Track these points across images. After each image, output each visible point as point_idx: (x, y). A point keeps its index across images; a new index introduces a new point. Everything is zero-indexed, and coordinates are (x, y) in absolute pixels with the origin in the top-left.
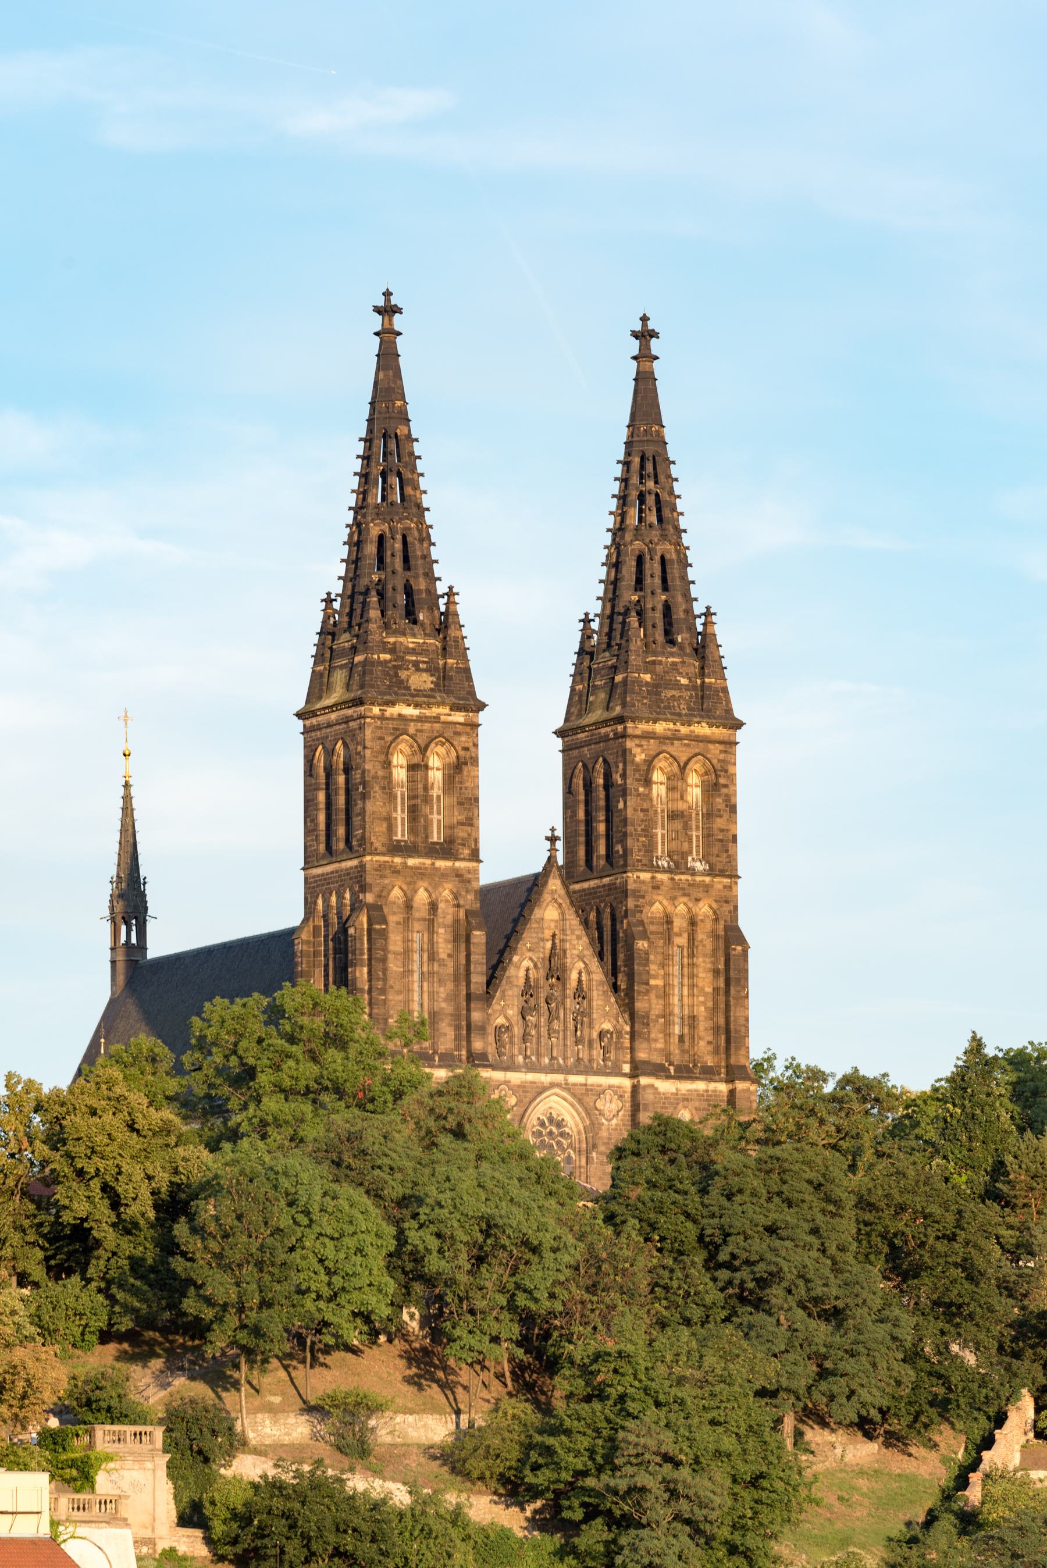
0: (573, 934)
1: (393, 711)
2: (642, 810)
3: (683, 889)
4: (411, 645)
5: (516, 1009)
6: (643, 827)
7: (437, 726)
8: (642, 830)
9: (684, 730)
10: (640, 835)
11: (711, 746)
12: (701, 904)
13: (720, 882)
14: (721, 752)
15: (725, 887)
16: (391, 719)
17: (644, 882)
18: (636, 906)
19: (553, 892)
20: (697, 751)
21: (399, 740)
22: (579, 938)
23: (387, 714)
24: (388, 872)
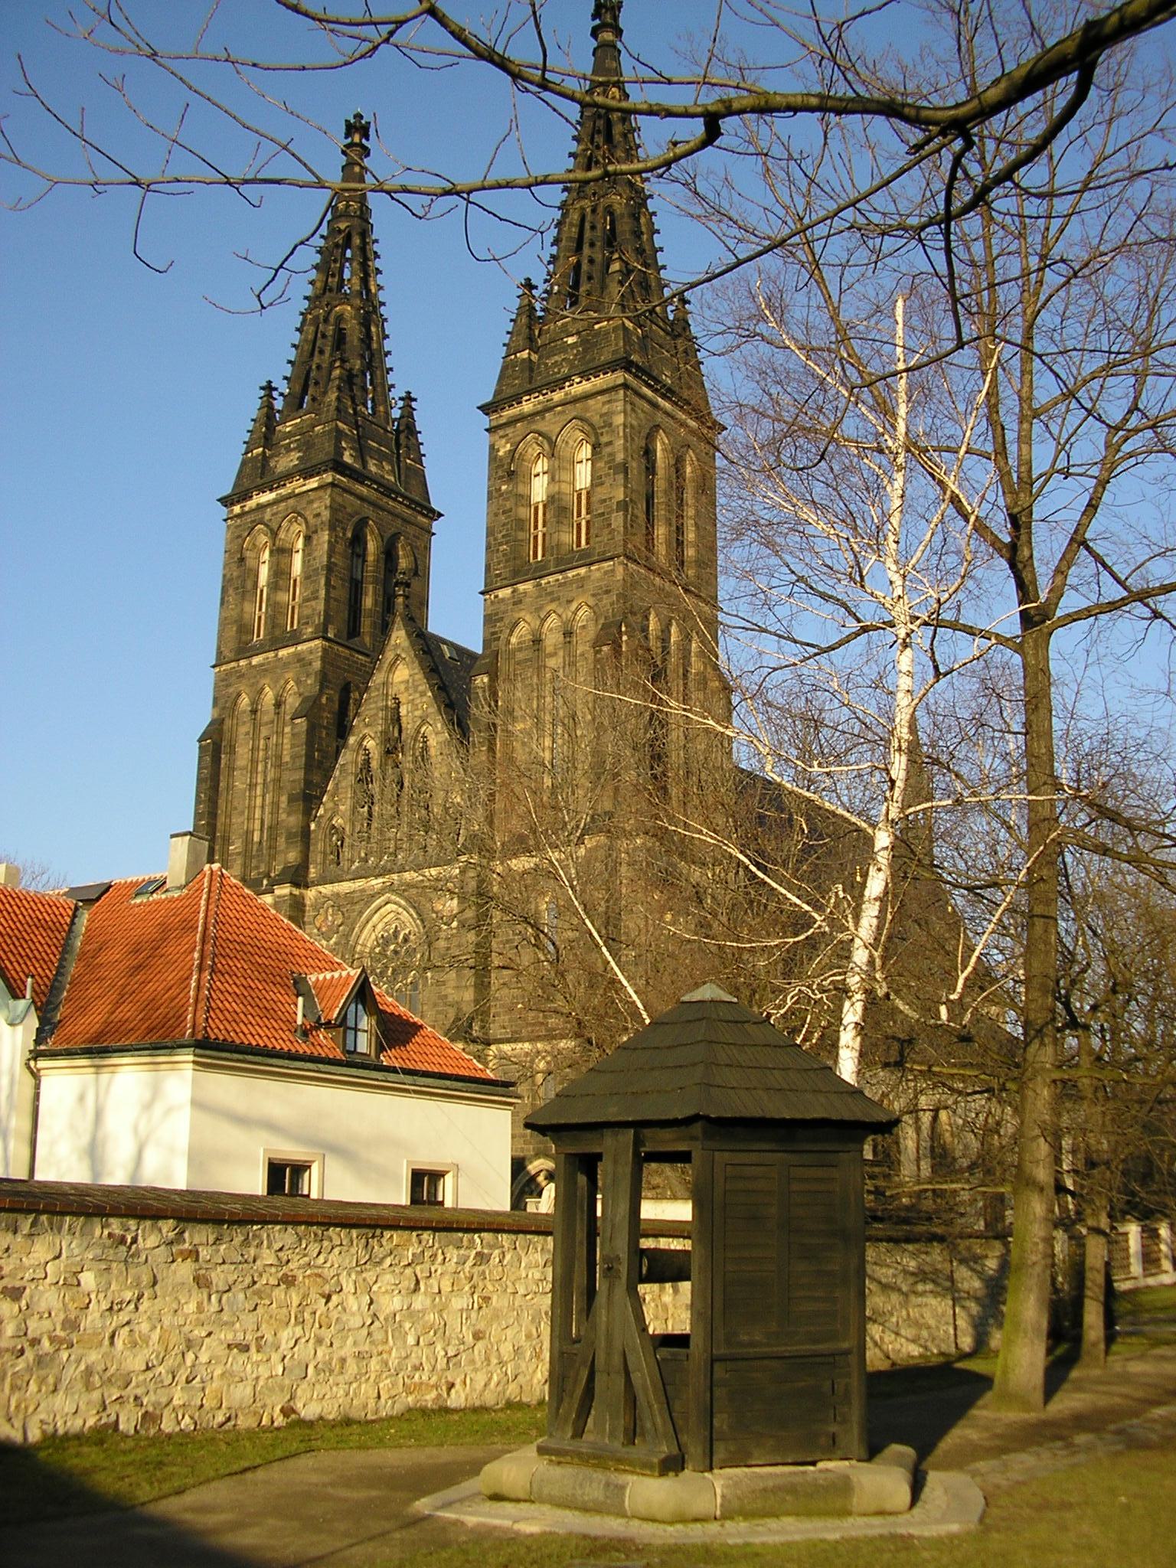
0: (416, 691)
1: (251, 504)
2: (504, 512)
3: (552, 593)
4: (288, 429)
5: (348, 802)
6: (504, 533)
7: (291, 501)
8: (503, 536)
9: (558, 396)
10: (501, 544)
11: (591, 402)
12: (574, 605)
13: (598, 569)
14: (604, 404)
15: (606, 573)
16: (251, 511)
17: (503, 600)
18: (493, 634)
19: (397, 646)
20: (574, 414)
21: (254, 532)
22: (423, 694)
23: (246, 509)
24: (233, 679)
